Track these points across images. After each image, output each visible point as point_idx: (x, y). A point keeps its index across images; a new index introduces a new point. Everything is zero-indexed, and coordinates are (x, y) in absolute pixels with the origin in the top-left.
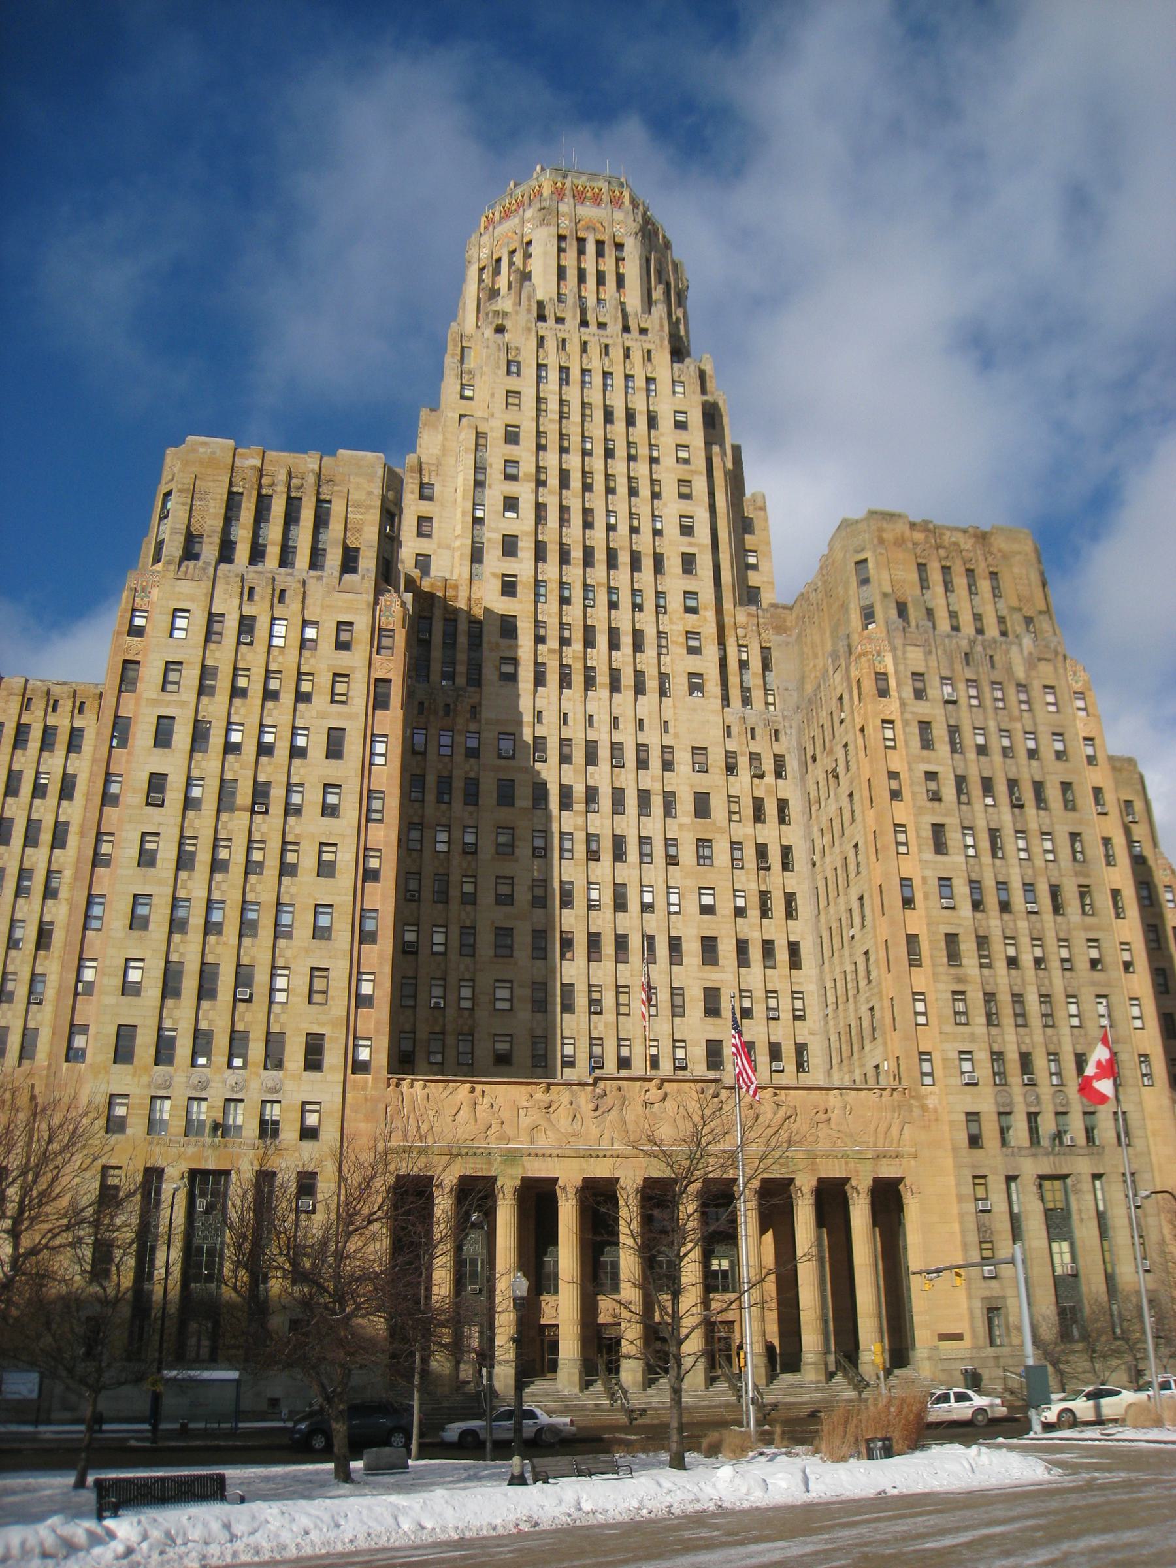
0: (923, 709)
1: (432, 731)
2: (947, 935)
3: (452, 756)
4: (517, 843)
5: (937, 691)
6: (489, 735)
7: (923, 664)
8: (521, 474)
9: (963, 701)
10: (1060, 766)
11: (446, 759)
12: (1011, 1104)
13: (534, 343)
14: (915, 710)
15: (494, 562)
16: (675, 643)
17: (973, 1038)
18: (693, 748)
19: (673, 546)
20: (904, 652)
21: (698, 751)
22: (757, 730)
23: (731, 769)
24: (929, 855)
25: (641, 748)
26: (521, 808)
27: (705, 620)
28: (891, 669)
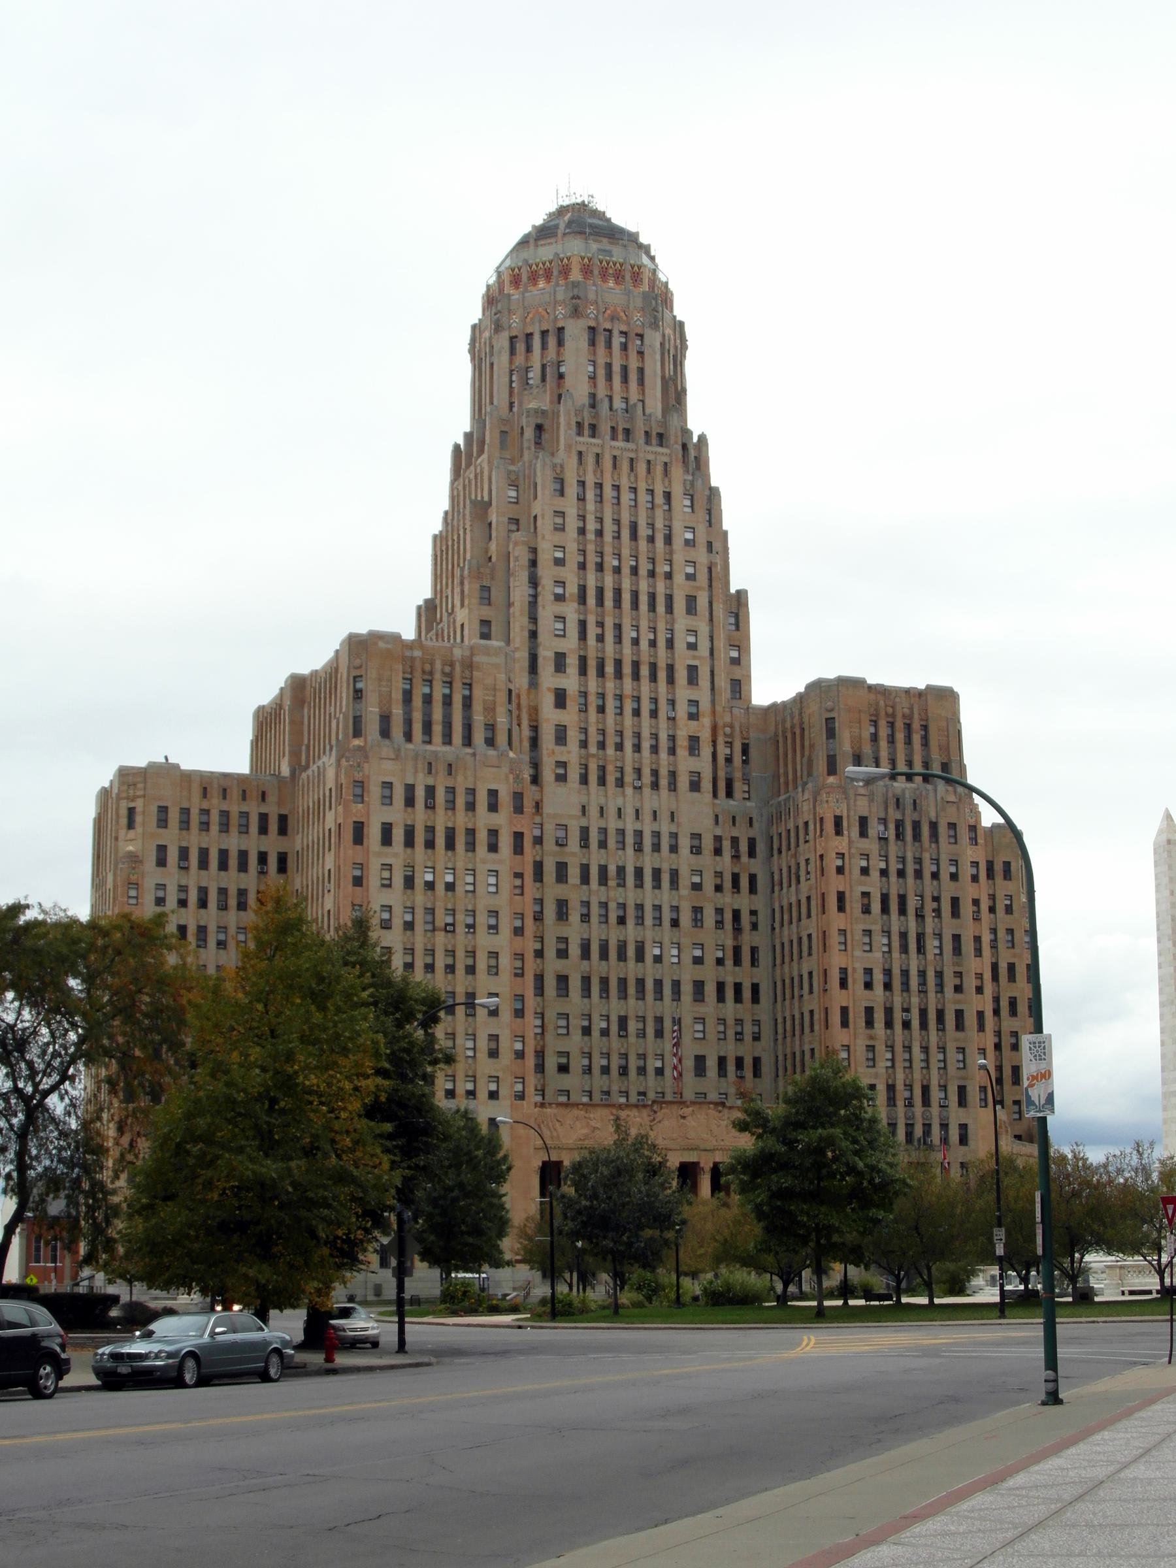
2: (866, 1008)
4: (570, 912)
5: (875, 829)
6: (549, 828)
10: (953, 884)
12: (896, 1118)
13: (574, 460)
15: (549, 679)
17: (876, 1076)
19: (683, 658)
20: (855, 800)
21: (696, 836)
22: (737, 818)
23: (718, 852)
24: (858, 953)
26: (574, 885)
27: (703, 726)
28: (845, 815)
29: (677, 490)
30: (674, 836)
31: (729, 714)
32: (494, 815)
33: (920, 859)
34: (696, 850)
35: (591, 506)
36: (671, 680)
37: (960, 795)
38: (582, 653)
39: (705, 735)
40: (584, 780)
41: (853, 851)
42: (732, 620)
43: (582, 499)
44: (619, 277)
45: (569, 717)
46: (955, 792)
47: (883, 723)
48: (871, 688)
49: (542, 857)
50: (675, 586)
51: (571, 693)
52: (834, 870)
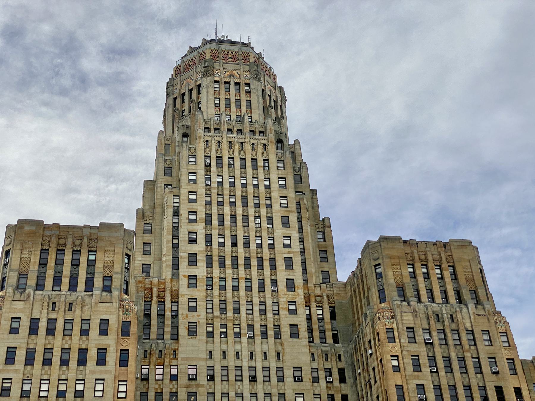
0: (414, 348)
1: (152, 367)
3: (163, 380)
5: (421, 337)
7: (413, 322)
8: (198, 219)
9: (436, 342)
11: (160, 382)
14: (409, 349)
15: (184, 269)
16: (283, 308)
18: (294, 368)
19: (281, 254)
22: (329, 356)
23: (316, 380)
25: (266, 369)
27: (298, 295)
28: (395, 327)
29: (273, 158)
30: (280, 369)
31: (319, 288)
32: (104, 337)
33: (464, 358)
34: (298, 379)
35: (214, 168)
36: (273, 267)
37: (488, 311)
38: (209, 254)
39: (301, 300)
40: (210, 334)
41: (405, 353)
42: (321, 236)
43: (208, 166)
44: (235, 59)
45: (200, 292)
46: (484, 308)
47: (418, 265)
48: (405, 242)
49: (177, 389)
50: (273, 211)
51: (201, 277)
52: (391, 370)
